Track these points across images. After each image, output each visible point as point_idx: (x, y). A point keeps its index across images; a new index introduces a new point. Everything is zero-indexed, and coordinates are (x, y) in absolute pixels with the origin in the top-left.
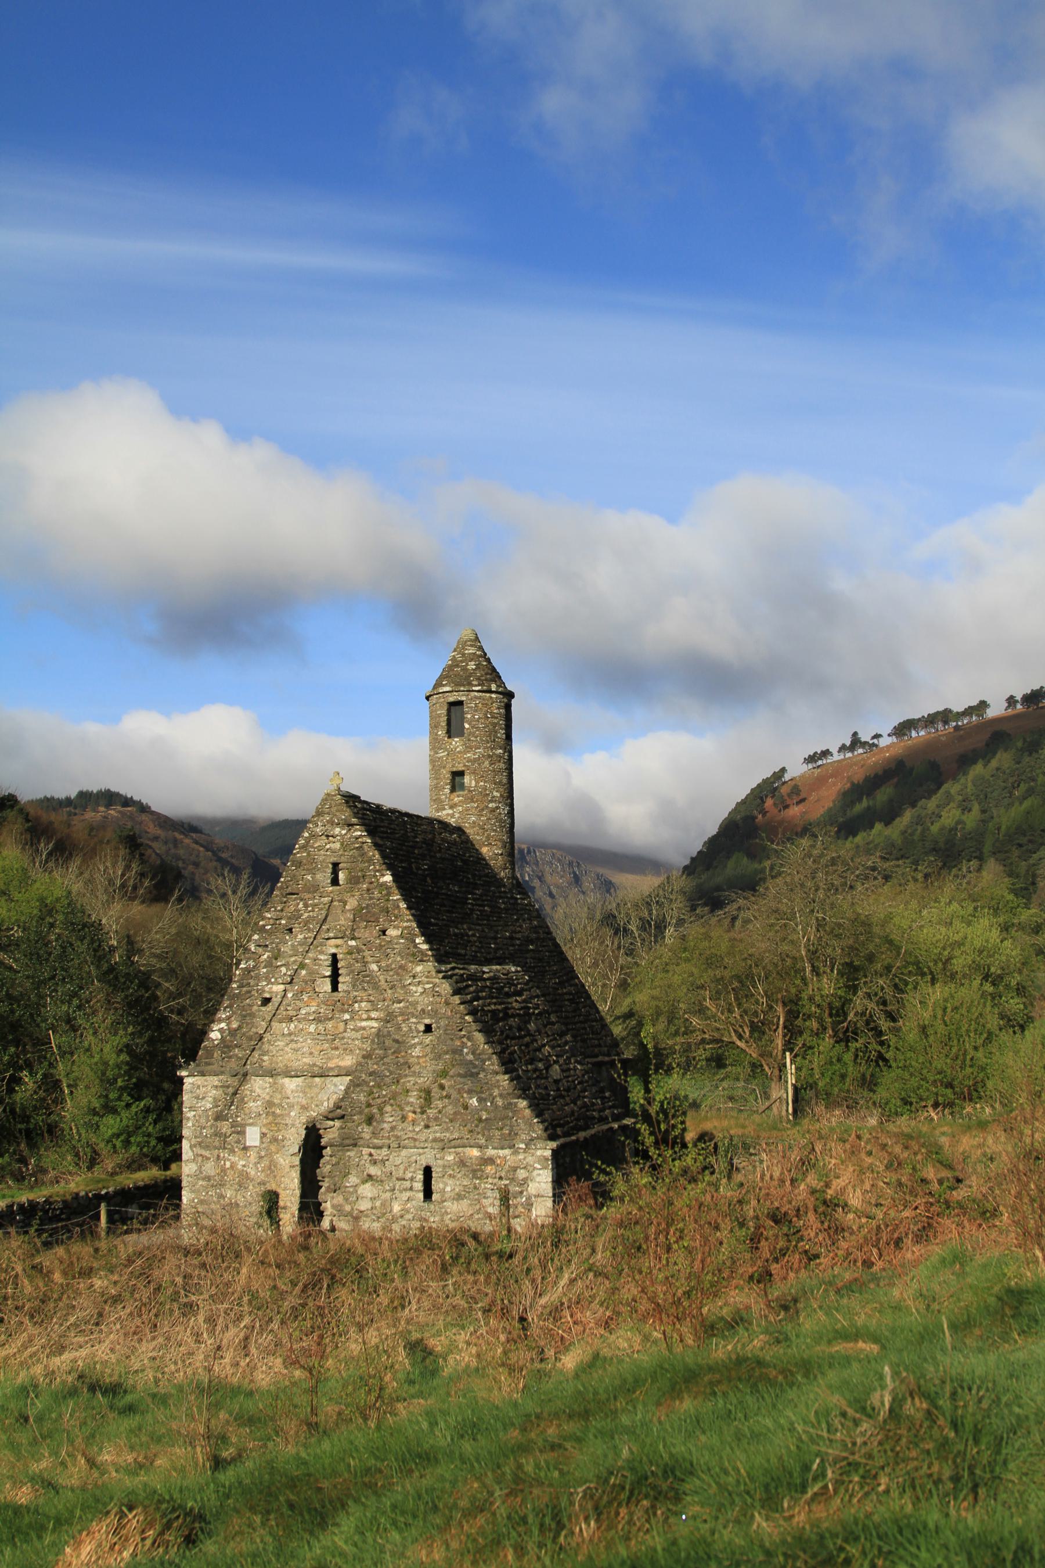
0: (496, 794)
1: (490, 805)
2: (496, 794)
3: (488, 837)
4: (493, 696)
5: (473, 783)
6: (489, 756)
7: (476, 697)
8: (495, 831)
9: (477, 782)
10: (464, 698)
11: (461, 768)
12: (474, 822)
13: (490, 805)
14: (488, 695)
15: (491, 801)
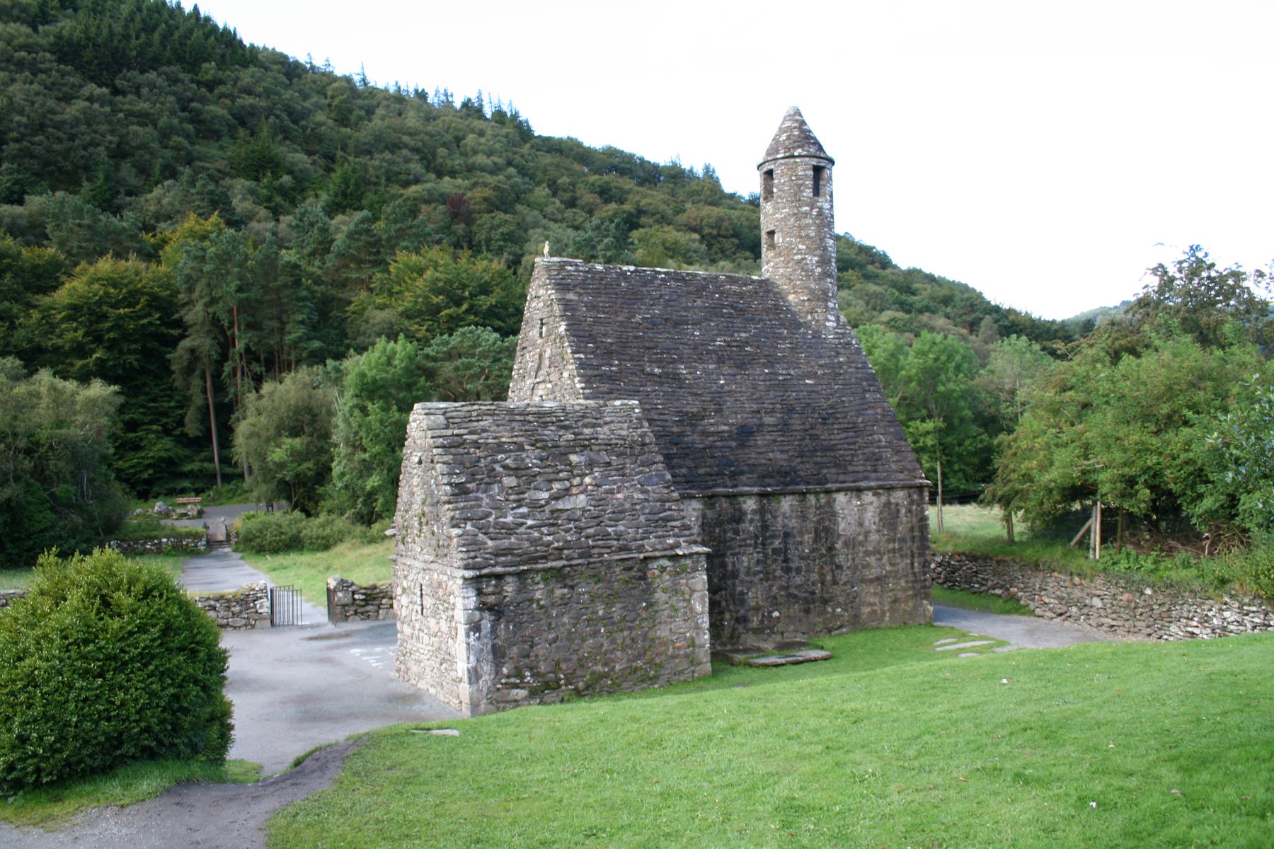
0: (801, 247)
1: (796, 257)
2: (801, 247)
3: (794, 287)
4: (798, 160)
5: (781, 240)
6: (795, 214)
7: (782, 164)
8: (802, 280)
9: (784, 239)
10: (772, 167)
11: (772, 228)
12: (782, 275)
13: (796, 257)
14: (792, 160)
15: (796, 254)
